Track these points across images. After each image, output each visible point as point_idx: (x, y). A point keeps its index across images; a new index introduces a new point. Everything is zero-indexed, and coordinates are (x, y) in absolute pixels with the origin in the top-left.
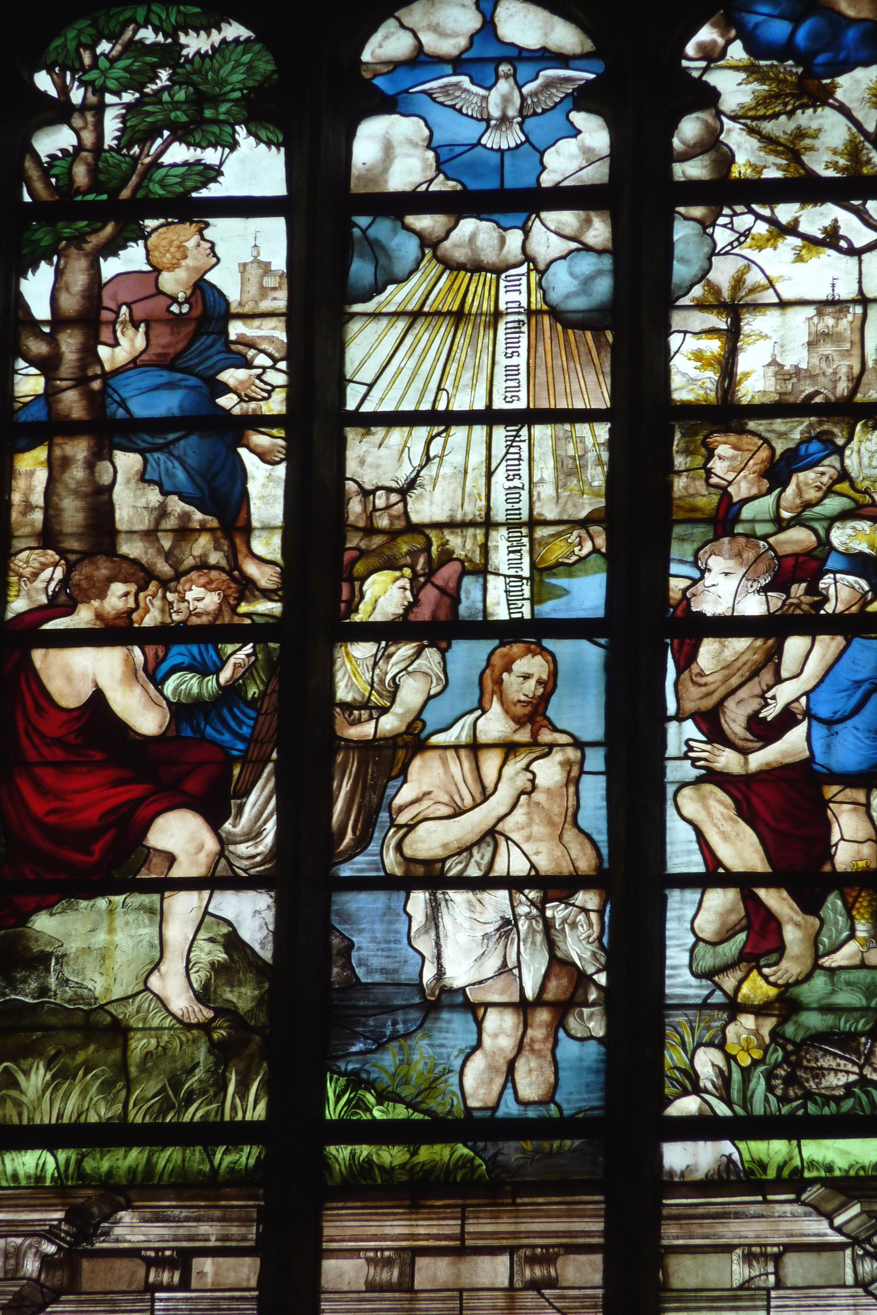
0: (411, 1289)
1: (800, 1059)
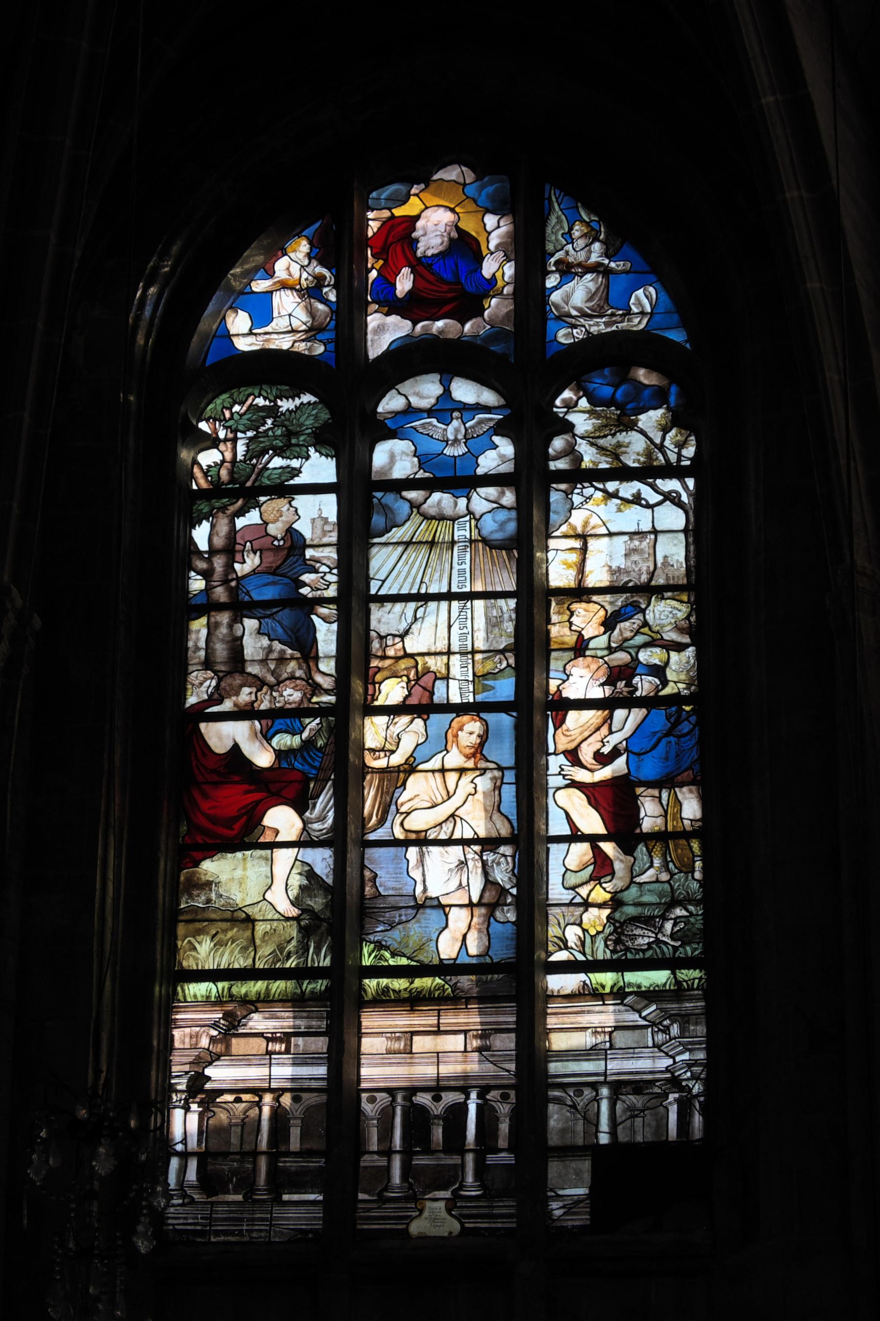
0: (411, 1053)
1: (623, 931)
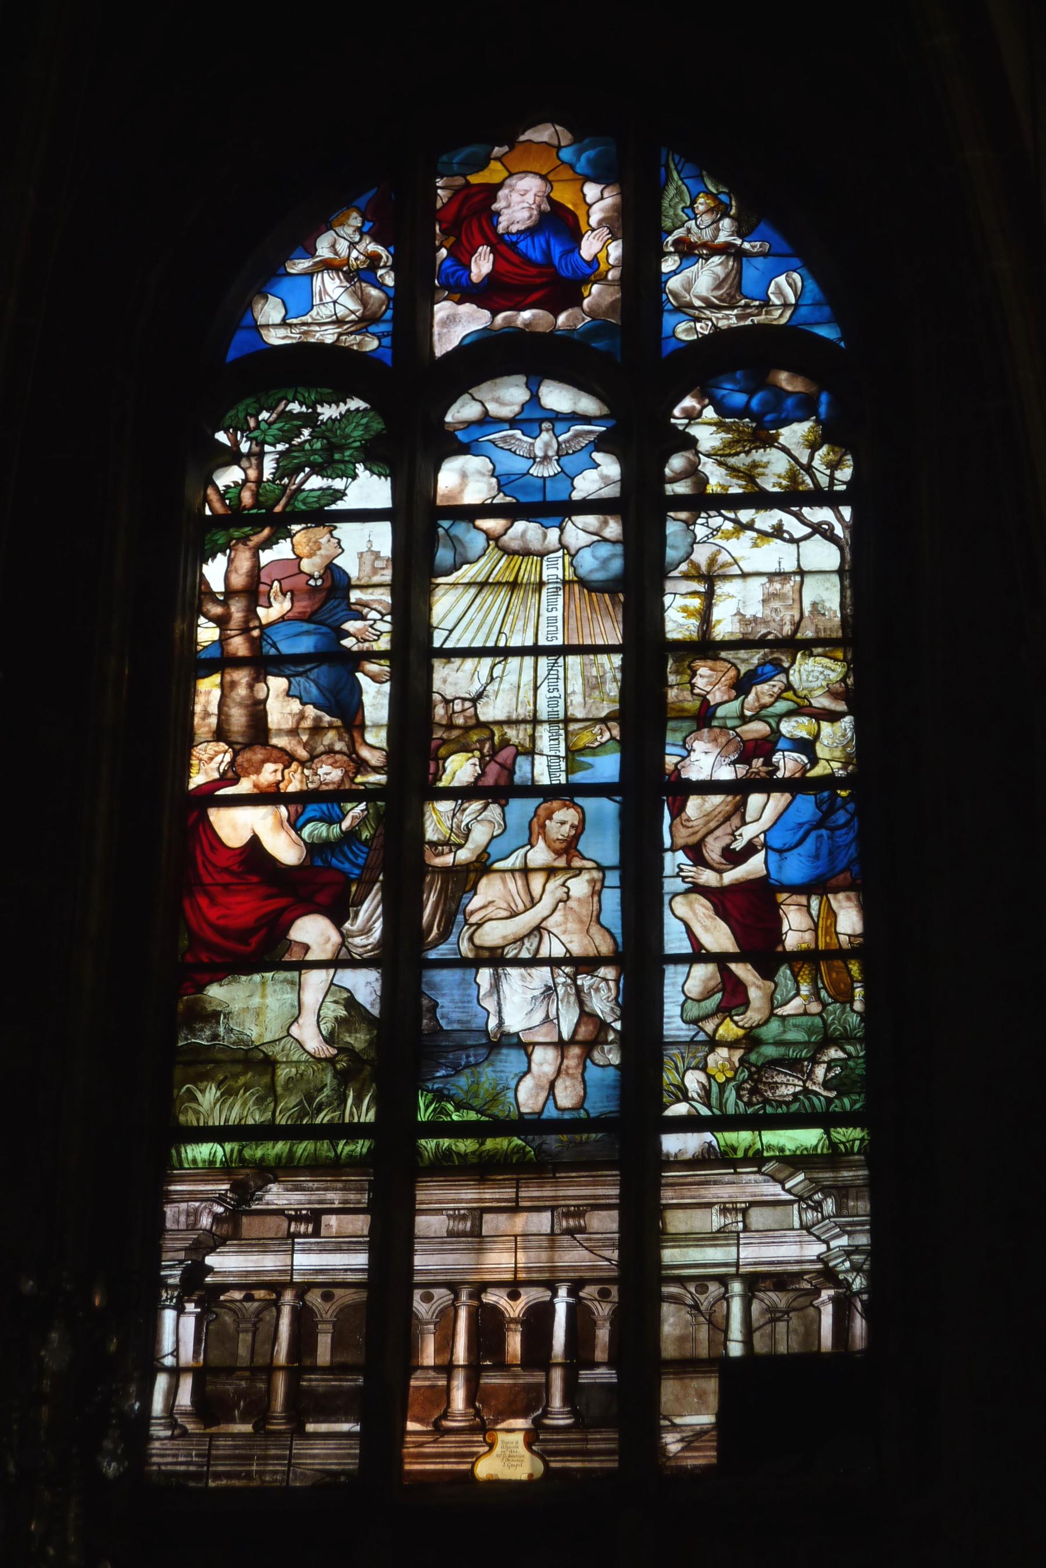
0: (480, 1235)
